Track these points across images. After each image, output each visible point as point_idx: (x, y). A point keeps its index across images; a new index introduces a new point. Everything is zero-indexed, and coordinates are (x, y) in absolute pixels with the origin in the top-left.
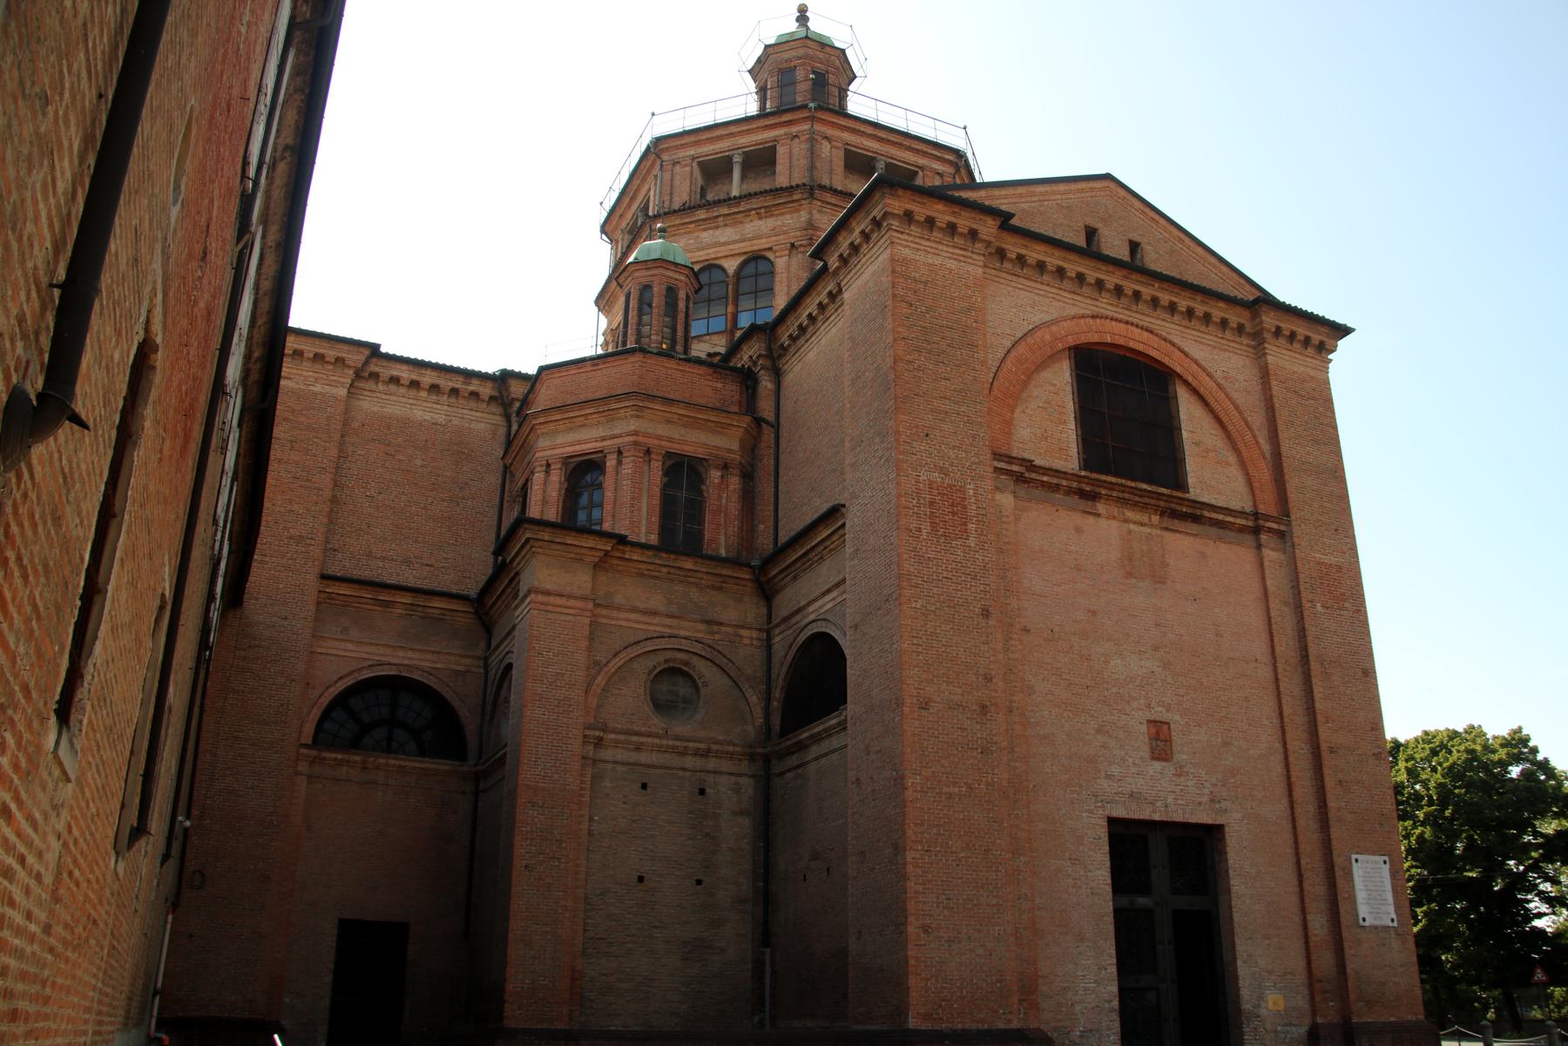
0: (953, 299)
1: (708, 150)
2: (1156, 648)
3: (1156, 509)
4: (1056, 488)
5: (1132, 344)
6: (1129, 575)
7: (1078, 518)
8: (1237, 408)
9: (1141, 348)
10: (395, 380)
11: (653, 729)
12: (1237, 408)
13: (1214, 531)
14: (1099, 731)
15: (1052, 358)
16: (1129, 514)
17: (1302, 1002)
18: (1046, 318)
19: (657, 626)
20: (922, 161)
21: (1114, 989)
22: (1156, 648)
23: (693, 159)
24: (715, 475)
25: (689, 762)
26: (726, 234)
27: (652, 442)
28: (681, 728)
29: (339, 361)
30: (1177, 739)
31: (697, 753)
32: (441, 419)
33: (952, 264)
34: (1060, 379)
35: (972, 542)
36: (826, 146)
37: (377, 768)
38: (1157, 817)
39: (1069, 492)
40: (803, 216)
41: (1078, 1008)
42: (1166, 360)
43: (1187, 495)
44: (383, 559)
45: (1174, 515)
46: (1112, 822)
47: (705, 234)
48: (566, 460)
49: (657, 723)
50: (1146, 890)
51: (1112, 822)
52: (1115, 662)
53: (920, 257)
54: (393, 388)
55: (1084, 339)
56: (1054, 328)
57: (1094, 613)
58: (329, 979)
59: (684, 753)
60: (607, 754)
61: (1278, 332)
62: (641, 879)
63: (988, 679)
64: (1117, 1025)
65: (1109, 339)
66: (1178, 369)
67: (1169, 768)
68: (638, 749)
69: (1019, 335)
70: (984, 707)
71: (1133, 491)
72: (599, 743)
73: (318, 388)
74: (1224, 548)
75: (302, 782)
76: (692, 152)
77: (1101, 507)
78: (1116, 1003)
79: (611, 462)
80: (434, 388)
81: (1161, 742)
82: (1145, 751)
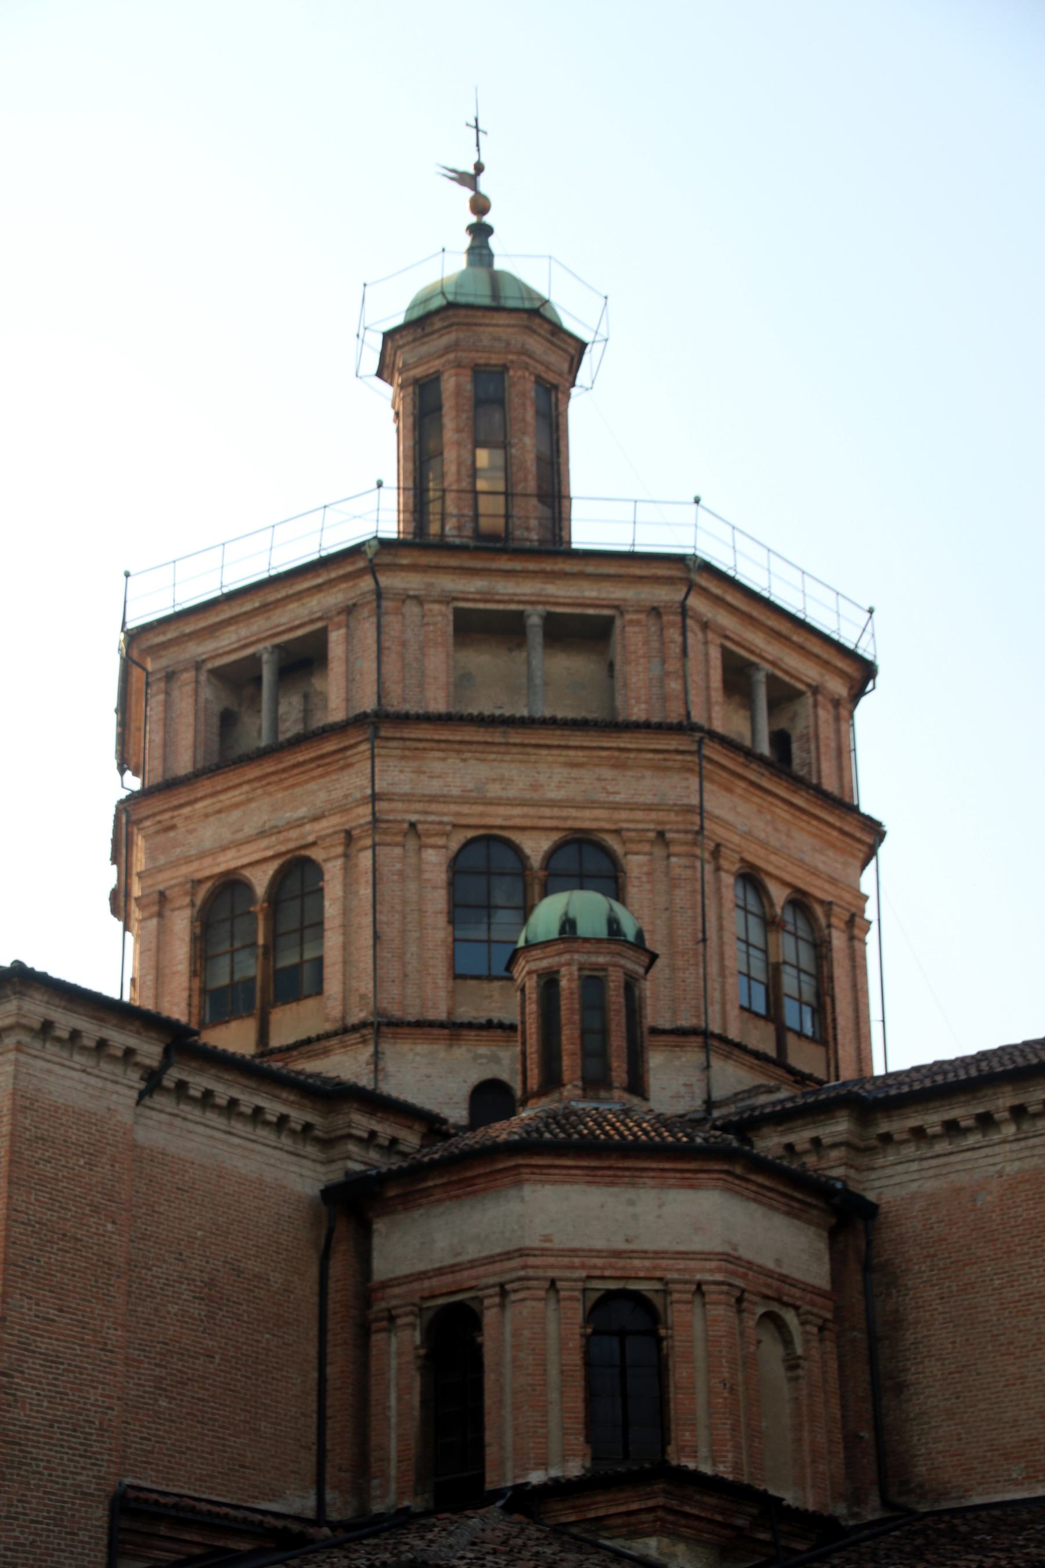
23: (198, 666)
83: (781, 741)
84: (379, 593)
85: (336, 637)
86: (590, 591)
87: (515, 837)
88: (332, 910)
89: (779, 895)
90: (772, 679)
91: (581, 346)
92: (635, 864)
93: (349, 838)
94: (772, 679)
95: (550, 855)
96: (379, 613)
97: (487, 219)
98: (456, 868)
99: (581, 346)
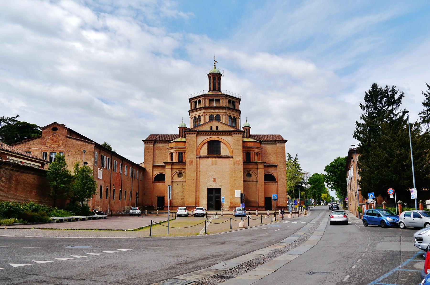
0: (192, 141)
1: (195, 100)
2: (215, 171)
3: (216, 157)
4: (204, 157)
5: (215, 139)
6: (212, 164)
7: (207, 160)
8: (229, 144)
9: (216, 139)
10: (158, 143)
11: (178, 179)
12: (228, 143)
13: (223, 158)
14: (207, 180)
15: (205, 143)
16: (213, 158)
17: (229, 204)
18: (204, 139)
19: (178, 170)
20: (220, 97)
21: (207, 203)
22: (215, 171)
23: (193, 102)
24: (184, 153)
25: (182, 182)
26: (196, 113)
27: (177, 151)
28: (181, 179)
29: (152, 143)
30: (216, 180)
31: (182, 181)
32: (163, 146)
33: (193, 137)
34: (206, 145)
35: (193, 165)
36: (207, 99)
37: (160, 182)
38: (213, 188)
39: (206, 157)
40: (203, 111)
41: (203, 204)
42: (219, 140)
43: (220, 155)
44: (159, 162)
45: (218, 157)
46: (208, 188)
47: (194, 113)
48: (171, 153)
49: (178, 179)
50: (212, 194)
51: (208, 188)
52: (210, 174)
53: (189, 137)
54: (158, 144)
55: (209, 140)
56: (205, 140)
57: (208, 169)
58: (157, 202)
59: (181, 181)
60: (174, 182)
61: (234, 134)
62: (177, 193)
63: (194, 177)
64: (207, 206)
65: (212, 140)
66: (221, 141)
67: (215, 183)
68: (176, 181)
69: (201, 142)
70: (194, 180)
71: (212, 156)
72: (173, 181)
73: (150, 146)
74: (225, 160)
75: (153, 185)
76: (193, 101)
77: (210, 158)
78: (207, 204)
79: (174, 153)
80: (162, 143)
81: (214, 181)
82: (212, 181)
83: (234, 105)
84: (204, 98)
85: (202, 101)
86: (219, 97)
87: (214, 115)
88: (201, 119)
89: (232, 117)
90: (232, 101)
91: (222, 74)
92: (221, 116)
93: (202, 115)
94: (232, 101)
95: (216, 115)
96: (204, 99)
97: (215, 64)
98: (209, 117)
99: (222, 74)
